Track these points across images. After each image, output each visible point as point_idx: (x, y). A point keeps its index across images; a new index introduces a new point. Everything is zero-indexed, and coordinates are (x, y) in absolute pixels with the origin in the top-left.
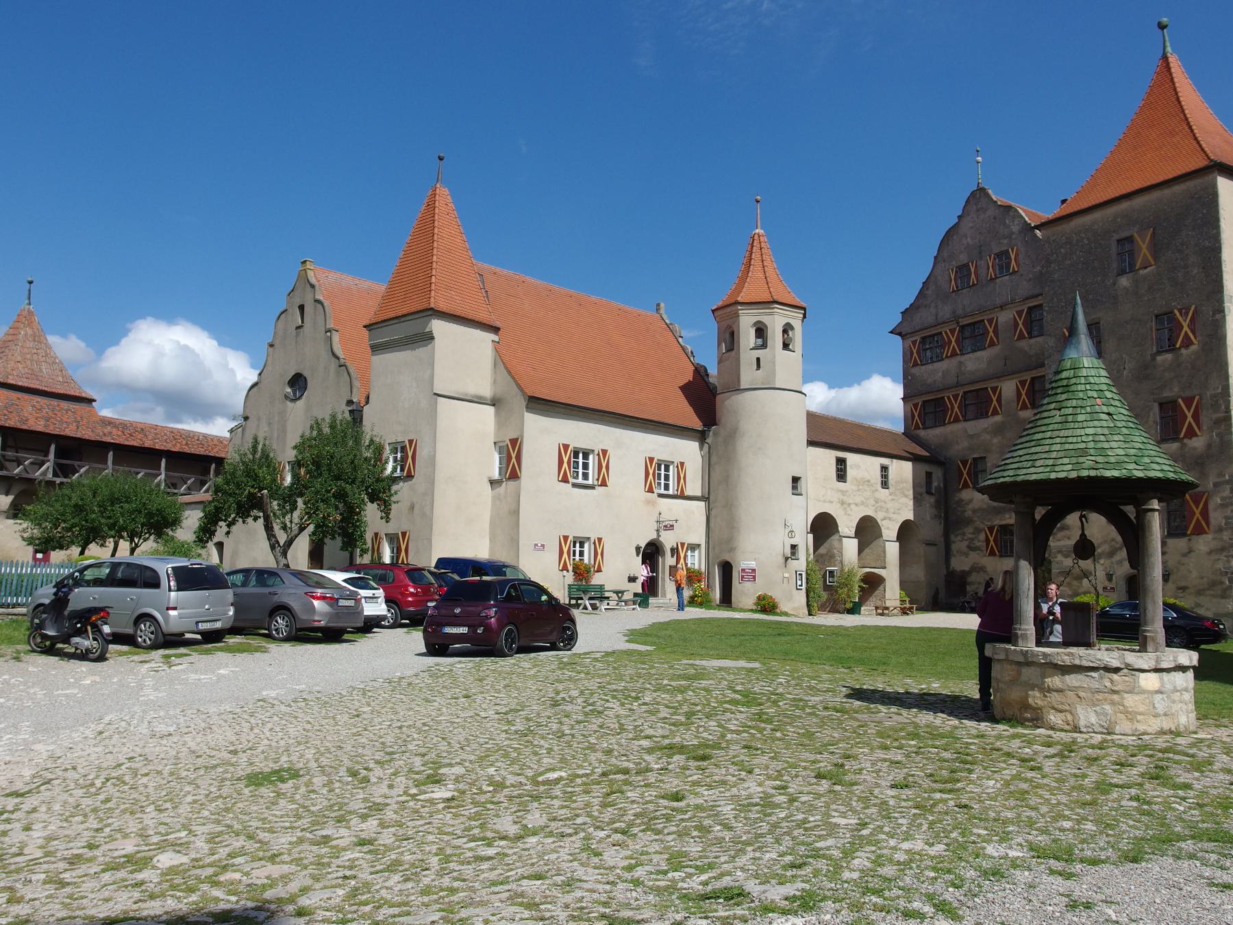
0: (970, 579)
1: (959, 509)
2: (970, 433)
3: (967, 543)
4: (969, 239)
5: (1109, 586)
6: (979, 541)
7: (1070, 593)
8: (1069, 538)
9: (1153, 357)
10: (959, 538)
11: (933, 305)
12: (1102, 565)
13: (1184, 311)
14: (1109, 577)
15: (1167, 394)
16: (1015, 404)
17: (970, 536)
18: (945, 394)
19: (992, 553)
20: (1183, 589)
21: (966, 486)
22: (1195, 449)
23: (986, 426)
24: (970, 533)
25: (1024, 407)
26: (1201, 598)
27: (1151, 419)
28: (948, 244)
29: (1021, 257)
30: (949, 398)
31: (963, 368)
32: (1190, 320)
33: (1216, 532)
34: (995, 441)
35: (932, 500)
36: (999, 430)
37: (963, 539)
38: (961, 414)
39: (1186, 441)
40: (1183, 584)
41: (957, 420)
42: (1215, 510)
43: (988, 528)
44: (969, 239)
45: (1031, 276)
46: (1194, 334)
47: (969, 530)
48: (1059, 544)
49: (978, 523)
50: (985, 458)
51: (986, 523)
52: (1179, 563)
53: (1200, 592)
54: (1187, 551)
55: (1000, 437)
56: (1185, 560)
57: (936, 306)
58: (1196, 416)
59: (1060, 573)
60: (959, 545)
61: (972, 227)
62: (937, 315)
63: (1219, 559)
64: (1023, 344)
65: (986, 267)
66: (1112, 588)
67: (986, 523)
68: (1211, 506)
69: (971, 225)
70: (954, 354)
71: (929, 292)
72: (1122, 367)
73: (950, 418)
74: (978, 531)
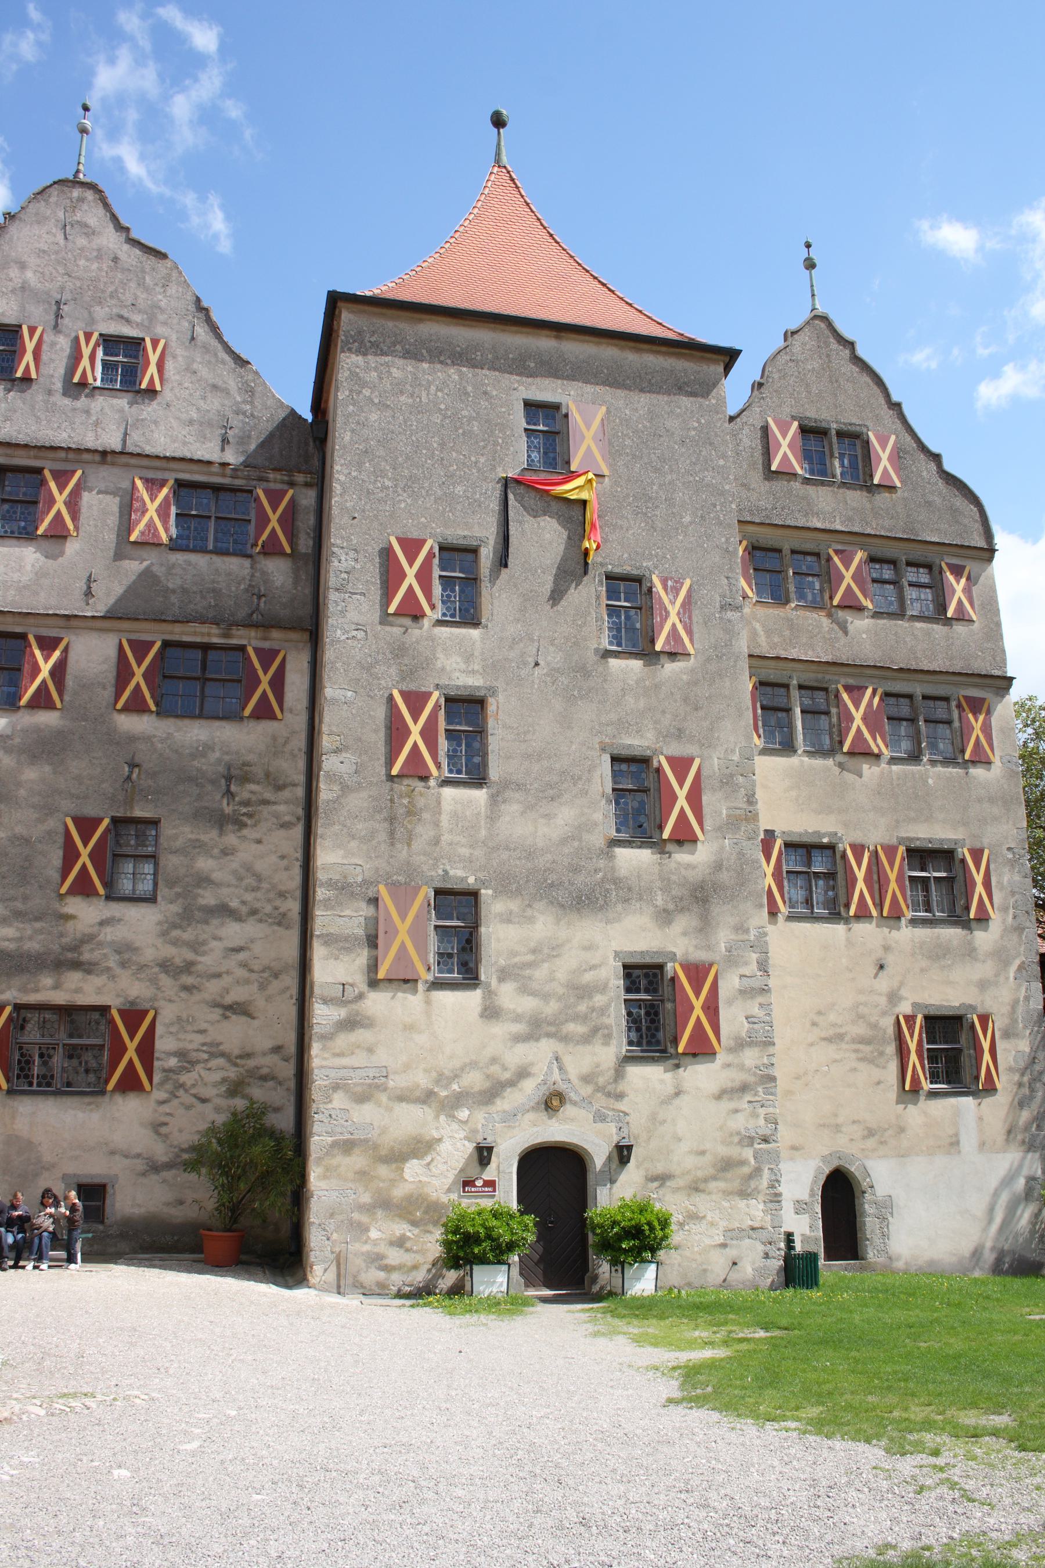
13: (670, 583)
15: (635, 743)
16: (109, 692)
20: (662, 1179)
32: (683, 605)
40: (660, 1168)
46: (690, 632)
55: (47, 768)
58: (695, 798)
59: (334, 1144)
63: (736, 1111)
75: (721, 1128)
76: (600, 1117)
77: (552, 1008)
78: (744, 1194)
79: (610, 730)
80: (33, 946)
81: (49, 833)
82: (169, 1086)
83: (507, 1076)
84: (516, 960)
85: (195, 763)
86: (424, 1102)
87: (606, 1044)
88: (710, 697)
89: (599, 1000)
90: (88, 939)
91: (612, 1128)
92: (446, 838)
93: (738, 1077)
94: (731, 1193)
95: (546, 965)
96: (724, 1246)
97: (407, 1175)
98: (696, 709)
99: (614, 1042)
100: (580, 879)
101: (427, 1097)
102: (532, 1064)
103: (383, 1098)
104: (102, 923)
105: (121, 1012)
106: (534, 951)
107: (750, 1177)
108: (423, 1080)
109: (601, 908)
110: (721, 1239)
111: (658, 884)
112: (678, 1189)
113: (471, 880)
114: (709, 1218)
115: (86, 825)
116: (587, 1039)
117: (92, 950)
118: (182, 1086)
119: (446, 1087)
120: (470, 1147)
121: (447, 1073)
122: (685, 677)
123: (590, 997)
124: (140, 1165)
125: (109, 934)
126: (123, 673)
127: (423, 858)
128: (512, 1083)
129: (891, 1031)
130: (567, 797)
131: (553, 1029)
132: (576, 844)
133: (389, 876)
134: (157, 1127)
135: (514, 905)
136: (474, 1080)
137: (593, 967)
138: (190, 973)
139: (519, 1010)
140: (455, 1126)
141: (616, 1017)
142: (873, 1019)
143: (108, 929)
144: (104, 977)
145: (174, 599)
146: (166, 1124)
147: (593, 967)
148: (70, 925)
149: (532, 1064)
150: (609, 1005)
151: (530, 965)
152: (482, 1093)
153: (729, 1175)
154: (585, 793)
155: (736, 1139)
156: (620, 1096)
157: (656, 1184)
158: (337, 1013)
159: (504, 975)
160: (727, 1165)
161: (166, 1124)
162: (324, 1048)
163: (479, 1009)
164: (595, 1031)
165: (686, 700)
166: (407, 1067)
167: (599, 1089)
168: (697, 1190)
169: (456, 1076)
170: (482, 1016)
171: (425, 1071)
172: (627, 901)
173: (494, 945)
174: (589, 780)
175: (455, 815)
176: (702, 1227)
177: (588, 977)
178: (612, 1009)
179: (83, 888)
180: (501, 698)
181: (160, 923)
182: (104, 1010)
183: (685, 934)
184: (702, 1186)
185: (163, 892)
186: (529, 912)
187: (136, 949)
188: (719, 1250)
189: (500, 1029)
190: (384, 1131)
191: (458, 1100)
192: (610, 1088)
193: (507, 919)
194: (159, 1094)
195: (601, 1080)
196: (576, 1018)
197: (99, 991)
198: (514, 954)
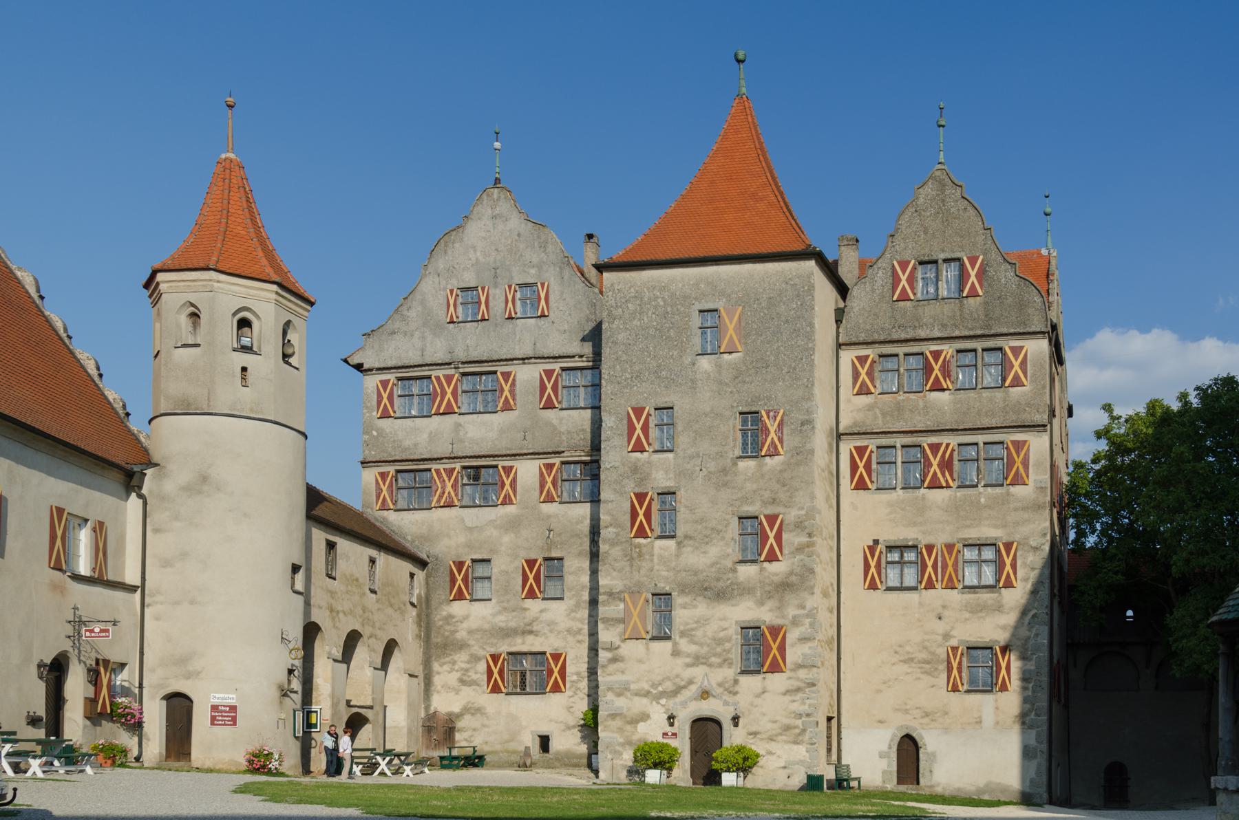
0: (459, 724)
1: (448, 628)
2: (469, 524)
3: (457, 675)
4: (479, 254)
5: (669, 730)
6: (476, 673)
7: (621, 740)
8: (623, 672)
9: (735, 464)
10: (446, 667)
11: (417, 334)
12: (663, 706)
14: (671, 719)
17: (464, 666)
18: (434, 466)
19: (495, 689)
20: (755, 734)
21: (460, 596)
22: (776, 574)
23: (493, 517)
24: (462, 662)
25: (549, 499)
26: (773, 743)
27: (729, 535)
28: (446, 252)
29: (552, 298)
30: (438, 471)
31: (461, 433)
32: (779, 425)
33: (792, 670)
34: (507, 539)
35: (414, 612)
36: (512, 525)
37: (452, 670)
38: (456, 495)
39: (766, 564)
40: (754, 729)
41: (450, 505)
42: (793, 645)
43: (491, 655)
44: (479, 254)
45: (566, 327)
47: (461, 658)
48: (609, 679)
49: (476, 648)
50: (488, 561)
51: (488, 649)
52: (752, 704)
53: (771, 739)
54: (760, 691)
55: (513, 535)
56: (758, 701)
57: (423, 338)
58: (778, 538)
60: (444, 676)
61: (484, 238)
62: (423, 350)
63: (794, 701)
64: (549, 414)
65: (504, 298)
66: (674, 734)
67: (488, 649)
68: (788, 641)
69: (483, 234)
70: (449, 412)
71: (412, 314)
72: (698, 469)
73: (439, 501)
74: (475, 659)
75: (785, 710)
76: (726, 703)
77: (704, 650)
78: (796, 743)
79: (737, 503)
80: (513, 624)
81: (516, 568)
82: (573, 689)
83: (683, 683)
84: (688, 627)
85: (579, 527)
86: (646, 696)
87: (730, 668)
88: (792, 478)
89: (727, 645)
90: (535, 619)
91: (732, 709)
92: (656, 567)
93: (797, 684)
94: (789, 742)
95: (702, 629)
96: (785, 768)
97: (639, 730)
98: (784, 486)
99: (734, 666)
100: (721, 584)
101: (647, 694)
102: (695, 678)
103: (628, 694)
104: (541, 611)
105: (550, 654)
106: (696, 622)
107: (799, 734)
108: (646, 687)
109: (729, 599)
110: (783, 765)
111: (758, 585)
112: (762, 739)
113: (667, 588)
114: (777, 754)
115: (531, 563)
116: (720, 666)
117: (537, 625)
118: (579, 689)
119: (656, 688)
120: (666, 716)
121: (656, 682)
122: (778, 468)
123: (723, 644)
124: (562, 727)
125: (546, 616)
126: (542, 484)
127: (645, 578)
128: (685, 687)
129: (944, 656)
130: (715, 541)
131: (704, 661)
132: (718, 566)
133: (630, 588)
134: (569, 708)
135: (687, 599)
136: (668, 686)
137: (725, 629)
138: (580, 634)
139: (689, 651)
140: (659, 706)
141: (735, 653)
142: (932, 649)
143: (544, 614)
144: (543, 637)
145: (564, 437)
146: (572, 707)
147: (725, 629)
148: (527, 613)
149: (695, 678)
150: (731, 648)
151: (692, 630)
152: (671, 692)
153: (788, 733)
154: (723, 538)
155: (793, 715)
156: (736, 693)
157: (752, 736)
158: (609, 655)
159: (683, 634)
160: (787, 728)
161: (572, 707)
162: (603, 672)
163: (670, 652)
164: (725, 660)
165: (778, 482)
166: (638, 680)
167: (726, 690)
168: (772, 740)
169: (660, 684)
170: (672, 655)
171: (647, 681)
172: (742, 595)
173: (678, 620)
174: (725, 532)
175: (661, 557)
176: (774, 758)
177: (722, 634)
178: (733, 650)
179: (531, 595)
180: (682, 492)
181: (566, 610)
182: (544, 653)
183: (771, 610)
184: (775, 738)
185: (567, 594)
186: (695, 602)
187: (556, 623)
188: (782, 770)
189: (680, 661)
190: (629, 709)
191: (663, 694)
192: (731, 689)
193: (684, 607)
194: (569, 693)
195: (727, 685)
196: (715, 655)
197: (541, 645)
198: (687, 624)
